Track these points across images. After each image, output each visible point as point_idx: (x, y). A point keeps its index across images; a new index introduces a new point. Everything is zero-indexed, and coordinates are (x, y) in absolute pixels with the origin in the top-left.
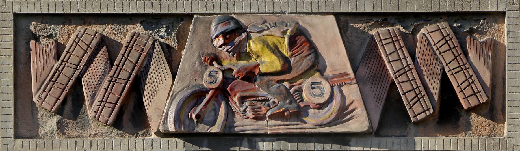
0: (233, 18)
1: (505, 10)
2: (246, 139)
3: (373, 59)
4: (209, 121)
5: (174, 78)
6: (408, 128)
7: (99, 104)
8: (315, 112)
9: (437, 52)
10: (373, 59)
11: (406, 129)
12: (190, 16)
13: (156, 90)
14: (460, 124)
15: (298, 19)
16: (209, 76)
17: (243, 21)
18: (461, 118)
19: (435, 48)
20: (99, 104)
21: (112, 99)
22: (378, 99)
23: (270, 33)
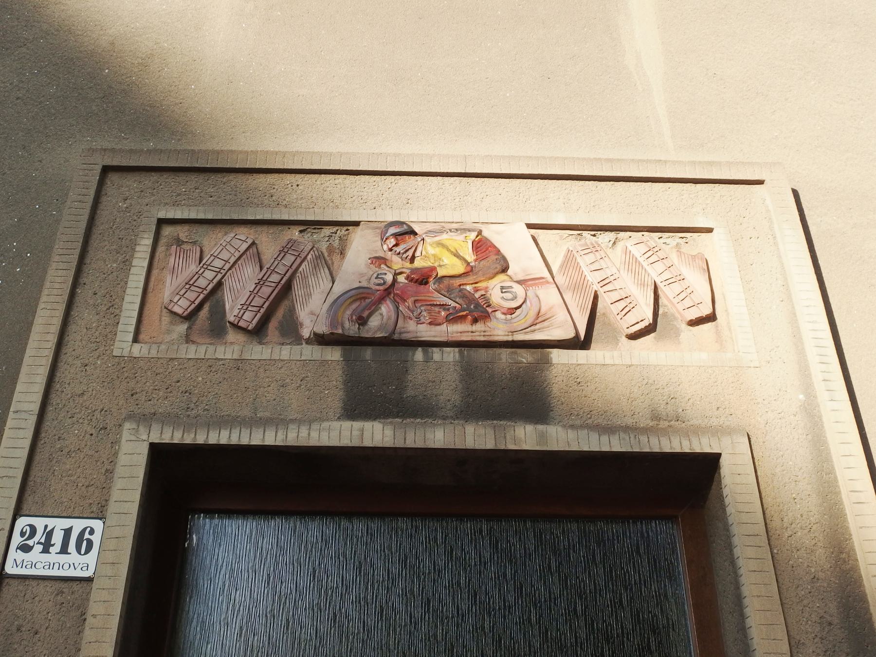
0: (406, 224)
1: (712, 227)
2: (420, 349)
3: (571, 269)
4: (374, 326)
5: (333, 283)
6: (620, 344)
7: (240, 307)
8: (506, 318)
9: (645, 264)
10: (571, 269)
11: (617, 344)
12: (356, 224)
13: (311, 294)
14: (680, 340)
15: (481, 227)
16: (376, 278)
17: (416, 228)
18: (682, 334)
19: (641, 260)
20: (240, 307)
21: (258, 301)
22: (582, 309)
23: (451, 238)
